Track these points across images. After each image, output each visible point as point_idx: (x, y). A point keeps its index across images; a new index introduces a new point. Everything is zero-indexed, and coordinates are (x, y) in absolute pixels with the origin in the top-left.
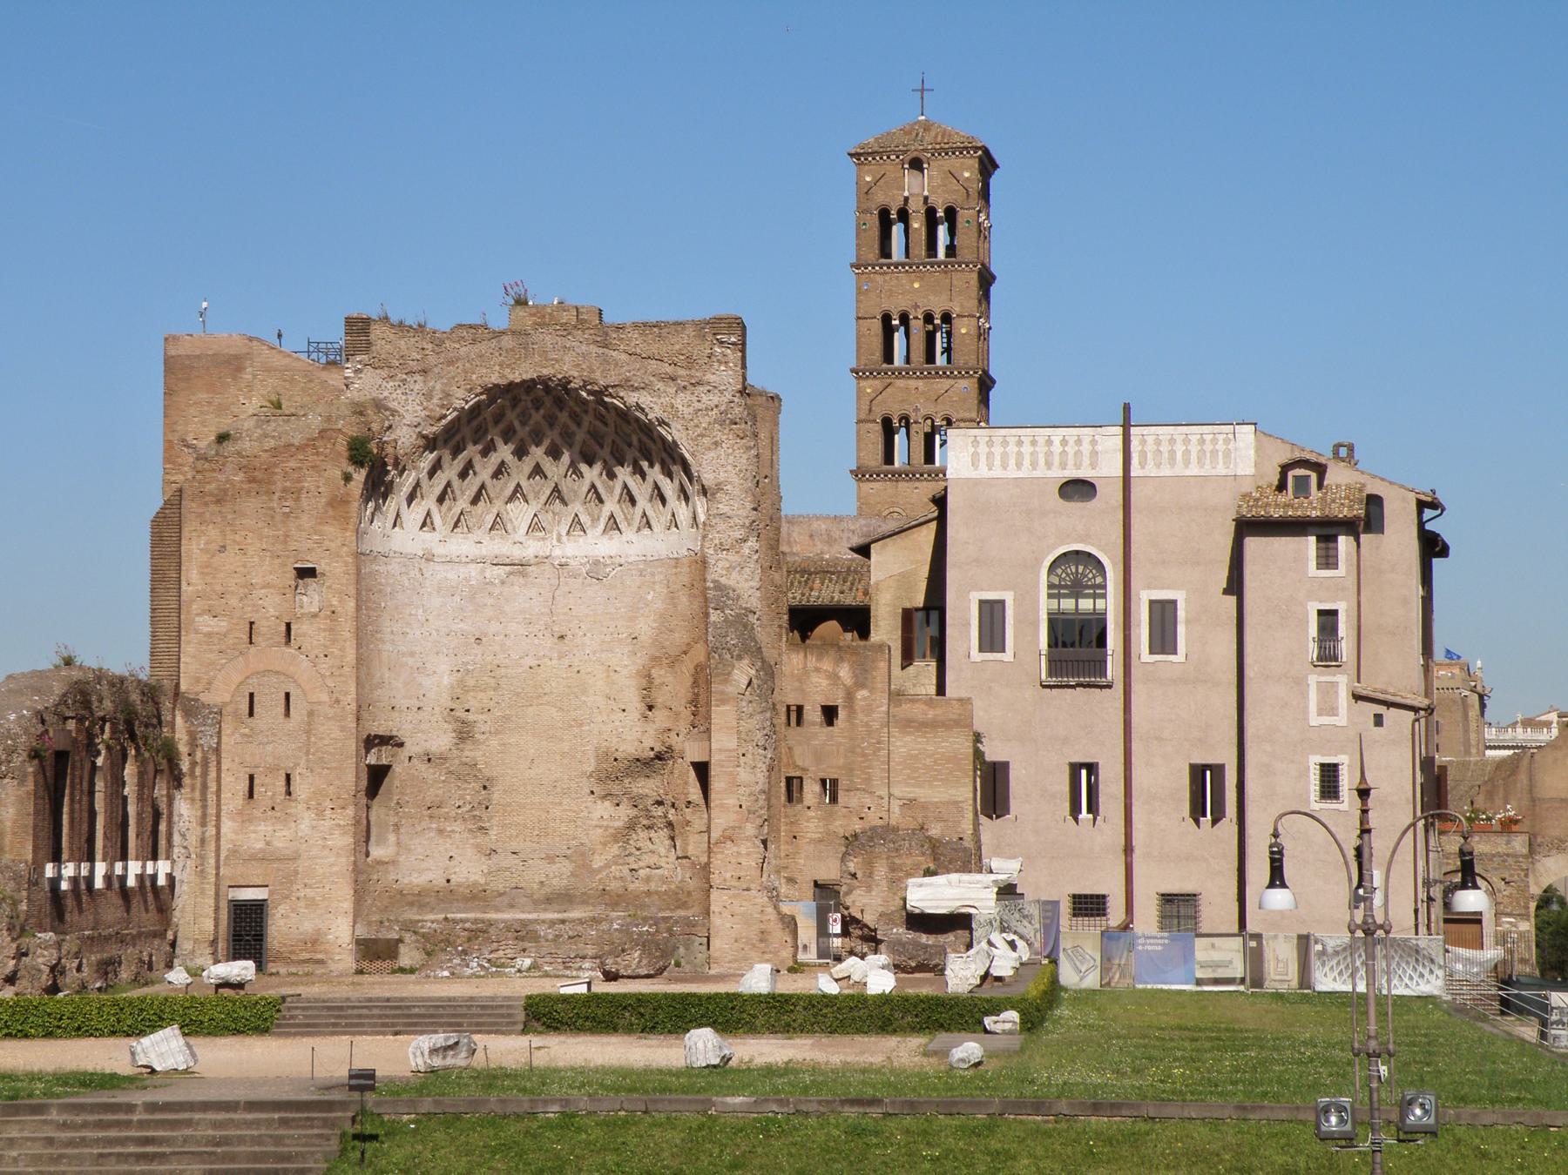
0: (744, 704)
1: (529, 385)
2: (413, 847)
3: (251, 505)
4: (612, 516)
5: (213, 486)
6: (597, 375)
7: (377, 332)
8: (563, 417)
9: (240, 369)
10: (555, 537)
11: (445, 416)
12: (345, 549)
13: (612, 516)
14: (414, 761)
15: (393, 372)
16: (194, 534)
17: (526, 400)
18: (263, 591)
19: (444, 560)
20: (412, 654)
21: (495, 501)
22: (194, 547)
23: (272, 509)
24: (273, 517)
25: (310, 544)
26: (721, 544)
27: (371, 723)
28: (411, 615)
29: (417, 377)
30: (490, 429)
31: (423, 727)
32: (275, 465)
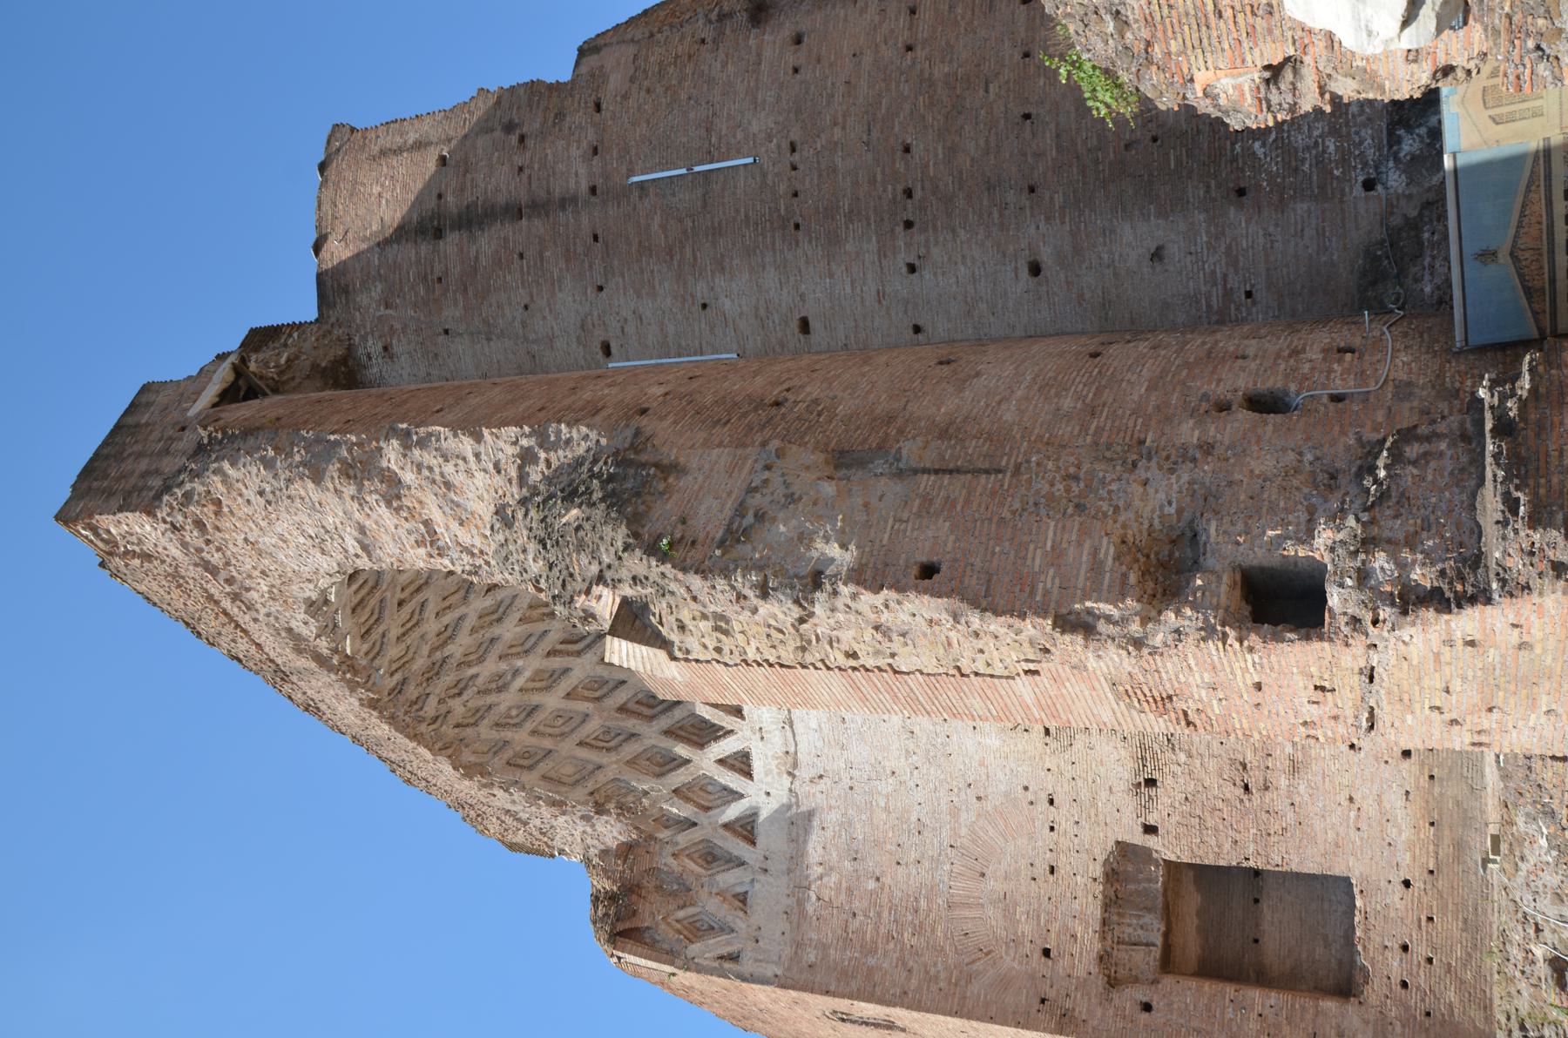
0: (692, 643)
2: (1331, 836)
14: (1151, 821)
19: (789, 734)
20: (955, 812)
26: (419, 544)
27: (1076, 950)
28: (887, 810)
30: (550, 710)
31: (1084, 795)
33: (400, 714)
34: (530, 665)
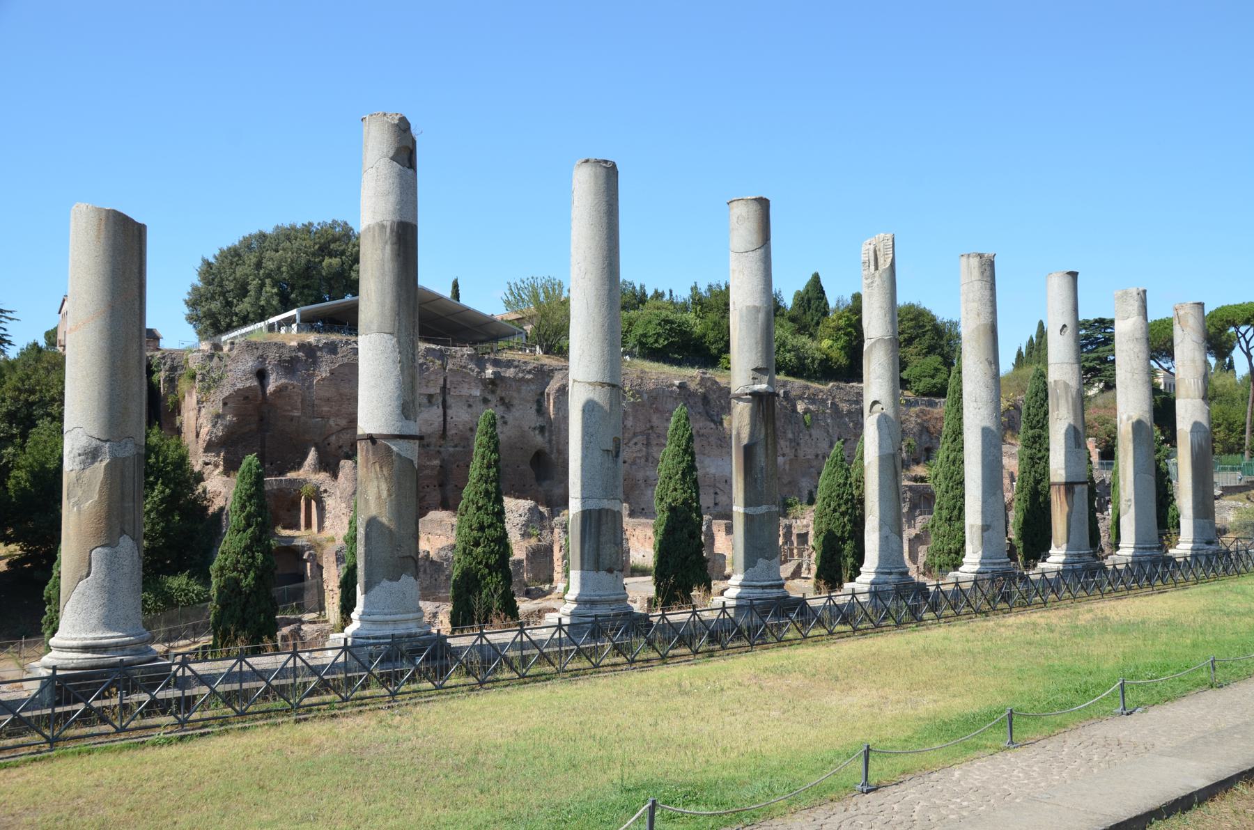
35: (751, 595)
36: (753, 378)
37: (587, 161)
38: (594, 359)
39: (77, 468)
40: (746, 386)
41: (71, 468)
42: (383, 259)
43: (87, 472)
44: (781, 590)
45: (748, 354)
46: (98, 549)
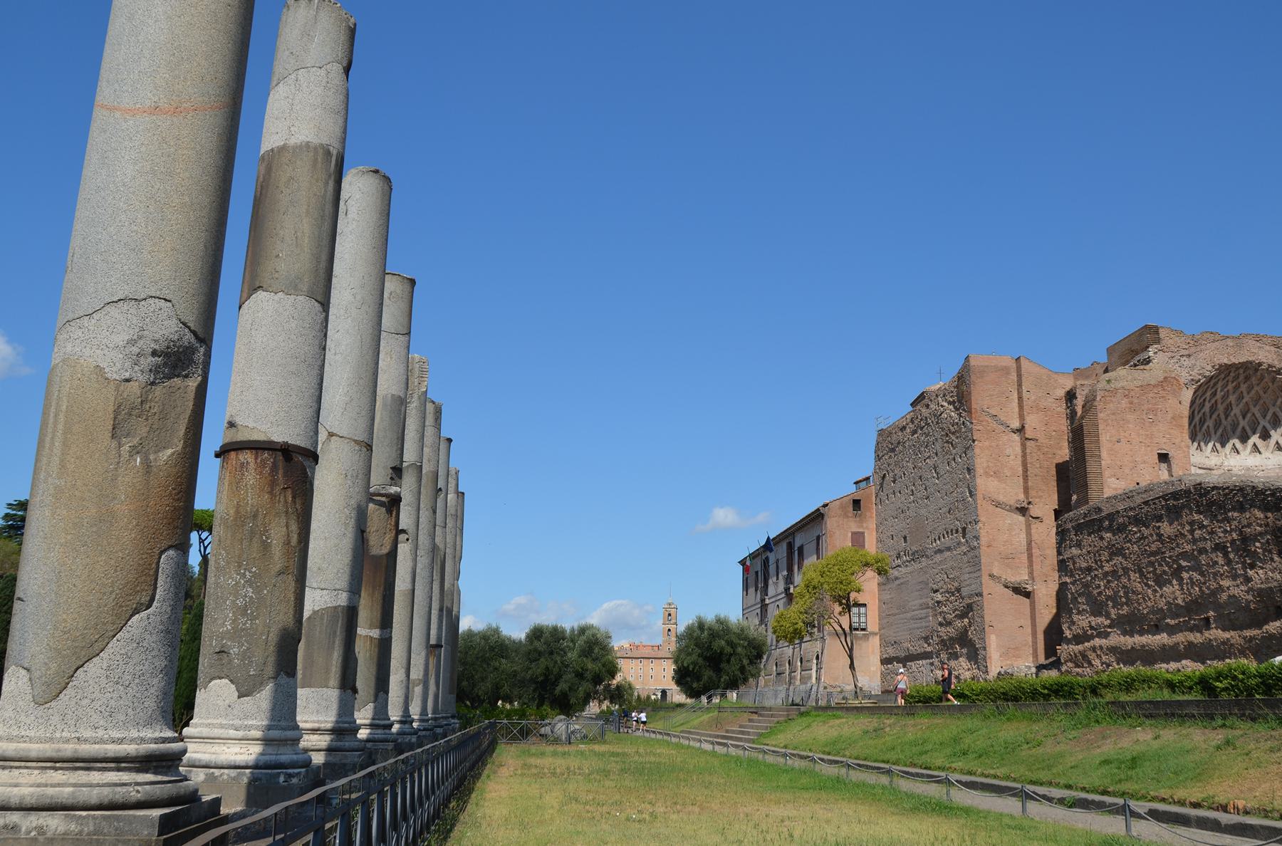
1: (1242, 364)
3: (1130, 417)
4: (1255, 444)
5: (1111, 405)
6: (1276, 363)
7: (1162, 334)
8: (1243, 387)
9: (1008, 373)
10: (1224, 454)
11: (1199, 380)
12: (1183, 443)
13: (1255, 444)
15: (1173, 354)
16: (1103, 431)
17: (1232, 374)
18: (1142, 465)
21: (1198, 434)
22: (1104, 439)
23: (1143, 419)
24: (1144, 424)
25: (1165, 440)
29: (1185, 358)
32: (1143, 395)
33: (1250, 365)
34: (1219, 395)
35: (376, 736)
36: (392, 478)
37: (376, 172)
38: (364, 413)
39: (143, 378)
40: (384, 485)
41: (127, 375)
42: (324, 197)
43: (158, 391)
44: (387, 731)
45: (388, 449)
46: (171, 552)
